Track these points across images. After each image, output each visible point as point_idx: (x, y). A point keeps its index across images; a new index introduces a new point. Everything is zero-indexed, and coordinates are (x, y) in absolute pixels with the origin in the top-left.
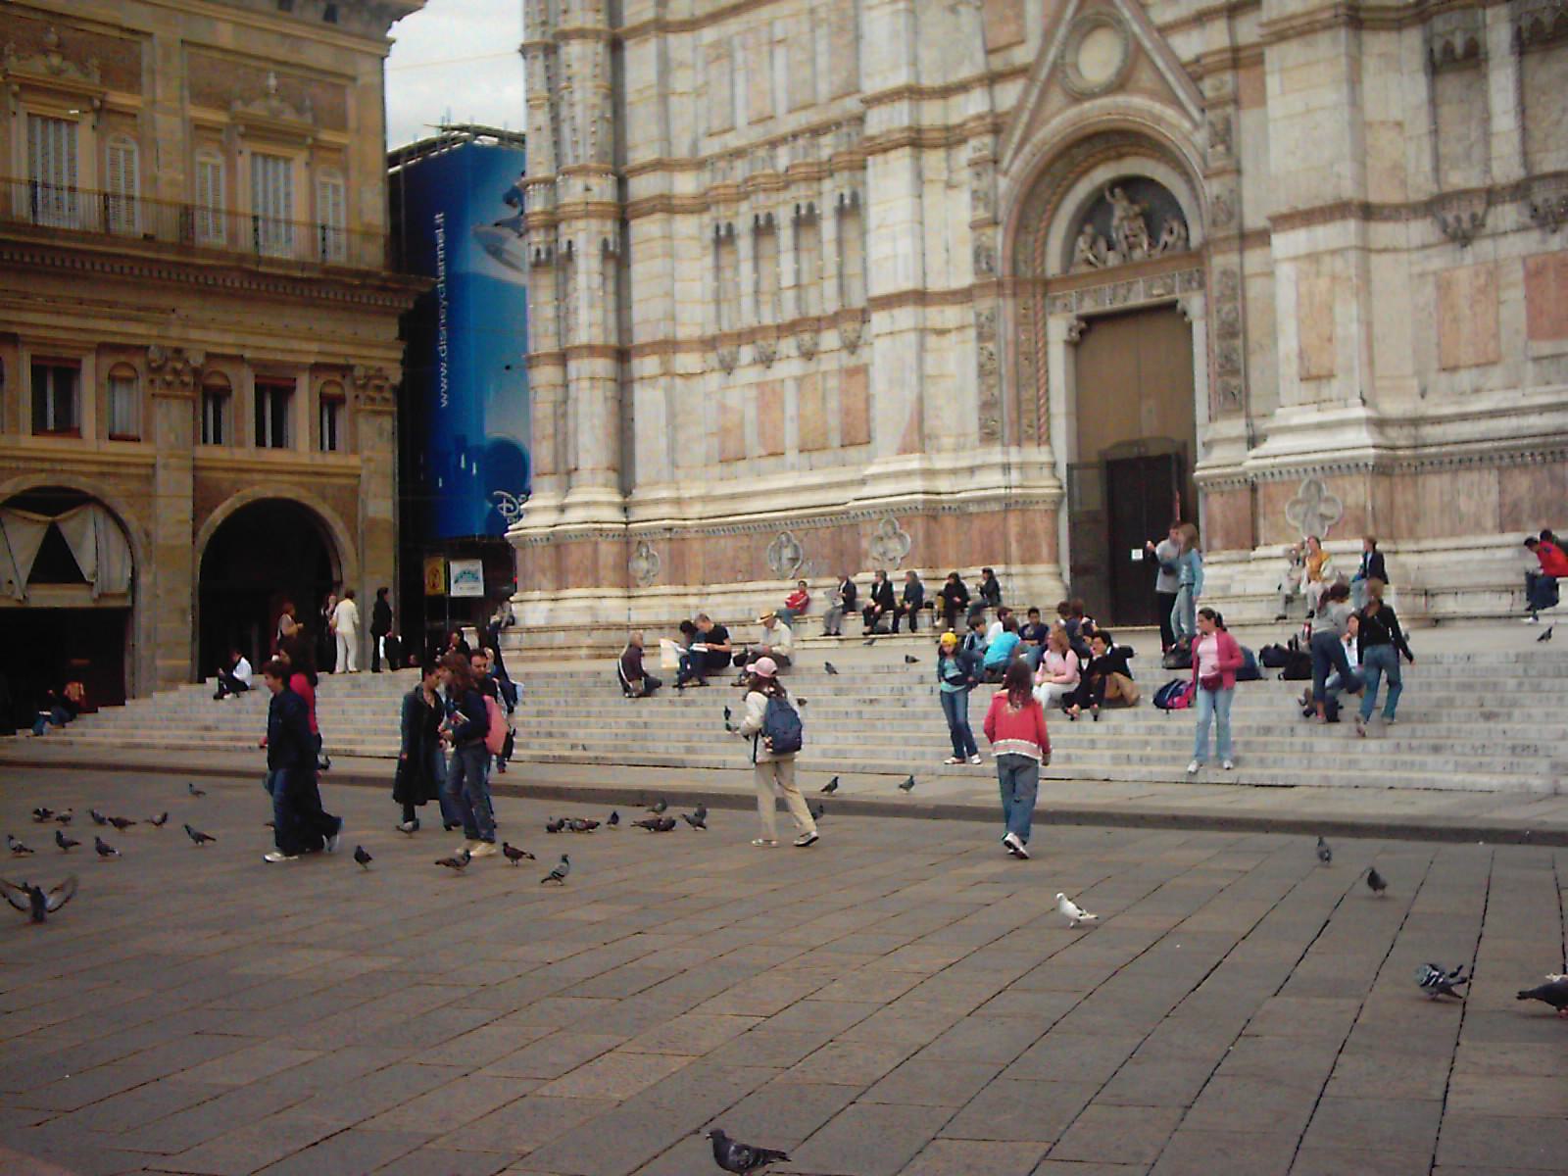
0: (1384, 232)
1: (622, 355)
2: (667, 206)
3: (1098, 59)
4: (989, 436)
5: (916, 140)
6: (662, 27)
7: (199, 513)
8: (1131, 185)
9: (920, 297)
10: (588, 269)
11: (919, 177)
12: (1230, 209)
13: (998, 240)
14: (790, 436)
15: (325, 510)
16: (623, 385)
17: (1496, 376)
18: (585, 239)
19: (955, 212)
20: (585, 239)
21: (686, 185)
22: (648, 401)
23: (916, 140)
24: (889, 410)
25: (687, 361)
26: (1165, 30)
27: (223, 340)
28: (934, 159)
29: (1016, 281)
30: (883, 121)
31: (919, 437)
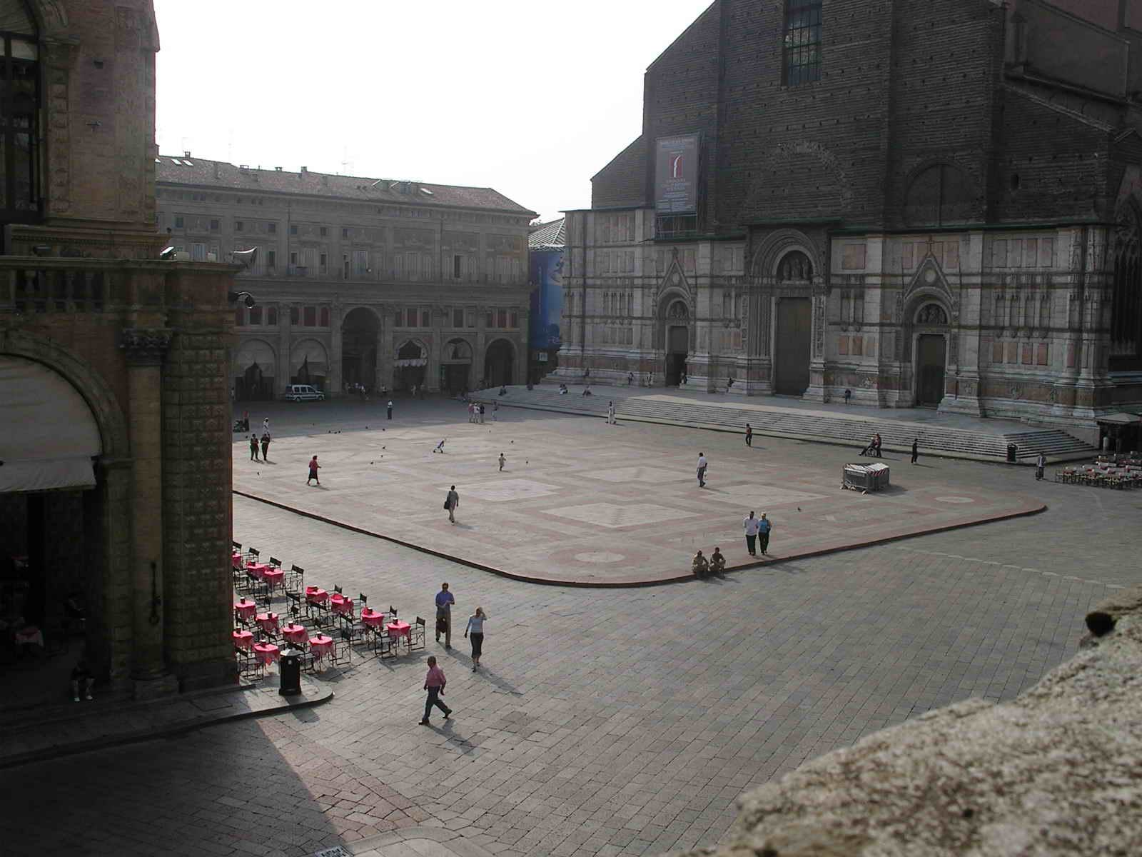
0: (714, 324)
1: (583, 317)
2: (594, 286)
3: (676, 279)
4: (653, 347)
6: (594, 247)
7: (487, 341)
8: (679, 302)
10: (576, 299)
11: (643, 294)
12: (694, 313)
13: (656, 309)
14: (617, 339)
15: (511, 340)
16: (583, 323)
17: (729, 351)
19: (650, 302)
21: (598, 282)
22: (588, 328)
23: (643, 287)
24: (636, 339)
26: (686, 277)
28: (646, 290)
29: (660, 317)
31: (641, 346)
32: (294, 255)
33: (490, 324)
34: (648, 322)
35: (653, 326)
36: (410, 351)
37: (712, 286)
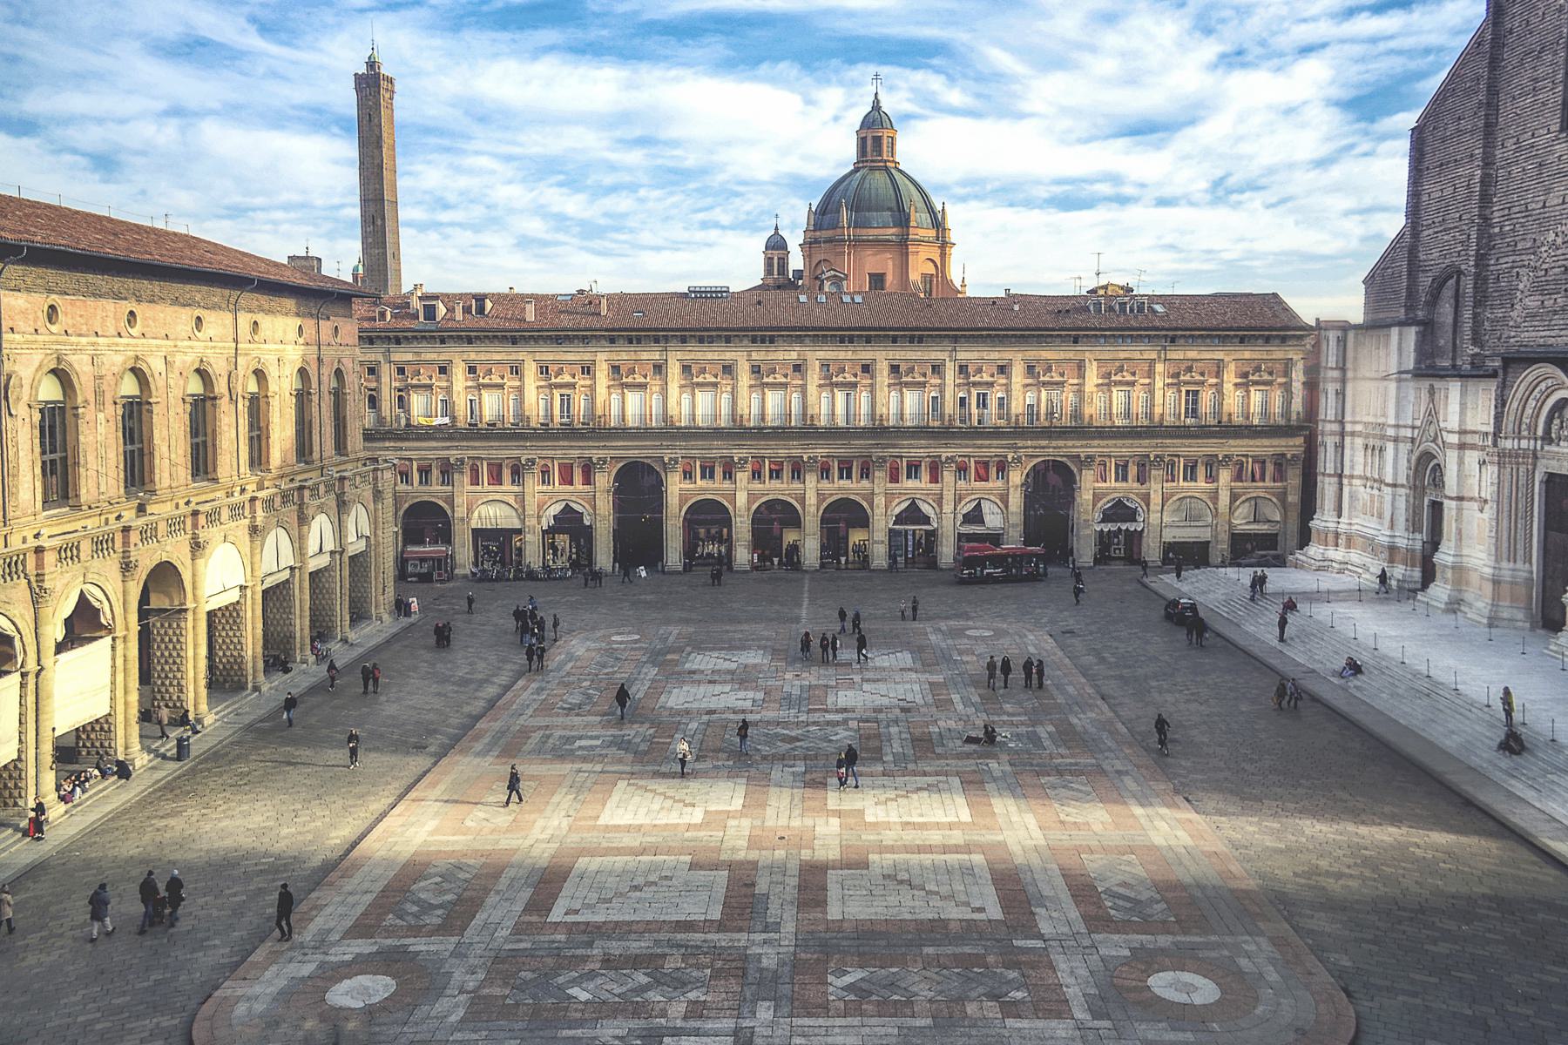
0: (1465, 504)
1: (1340, 476)
5: (1396, 440)
9: (1394, 485)
18: (1330, 441)
19: (1403, 463)
20: (1330, 441)
21: (1359, 428)
22: (1346, 490)
23: (1396, 440)
25: (1356, 482)
27: (1243, 451)
30: (1391, 432)
32: (962, 400)
33: (1238, 477)
34: (1403, 491)
35: (1407, 496)
36: (1120, 511)
37: (1462, 447)
